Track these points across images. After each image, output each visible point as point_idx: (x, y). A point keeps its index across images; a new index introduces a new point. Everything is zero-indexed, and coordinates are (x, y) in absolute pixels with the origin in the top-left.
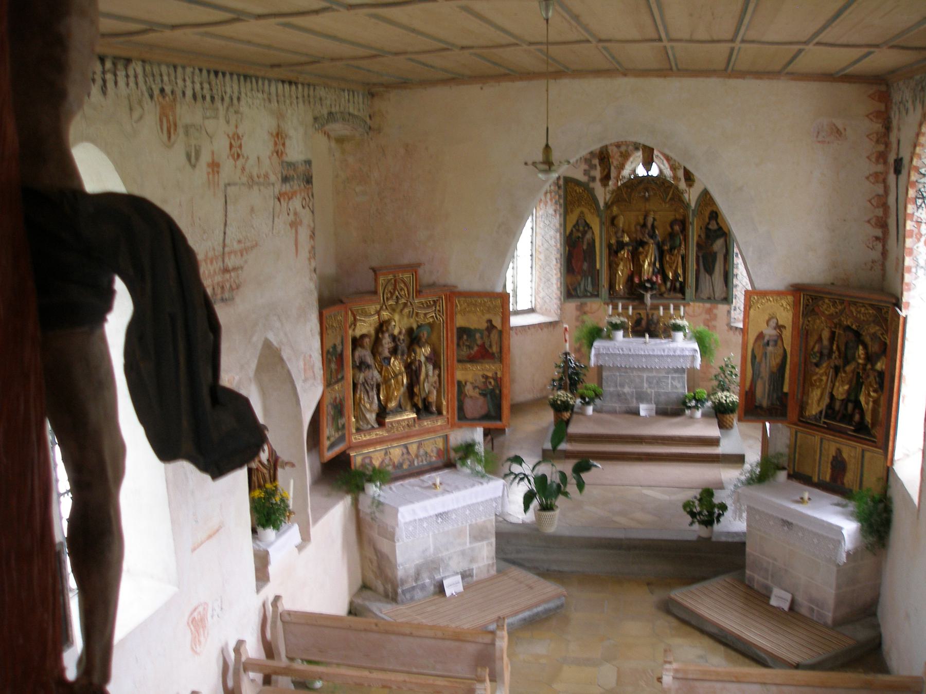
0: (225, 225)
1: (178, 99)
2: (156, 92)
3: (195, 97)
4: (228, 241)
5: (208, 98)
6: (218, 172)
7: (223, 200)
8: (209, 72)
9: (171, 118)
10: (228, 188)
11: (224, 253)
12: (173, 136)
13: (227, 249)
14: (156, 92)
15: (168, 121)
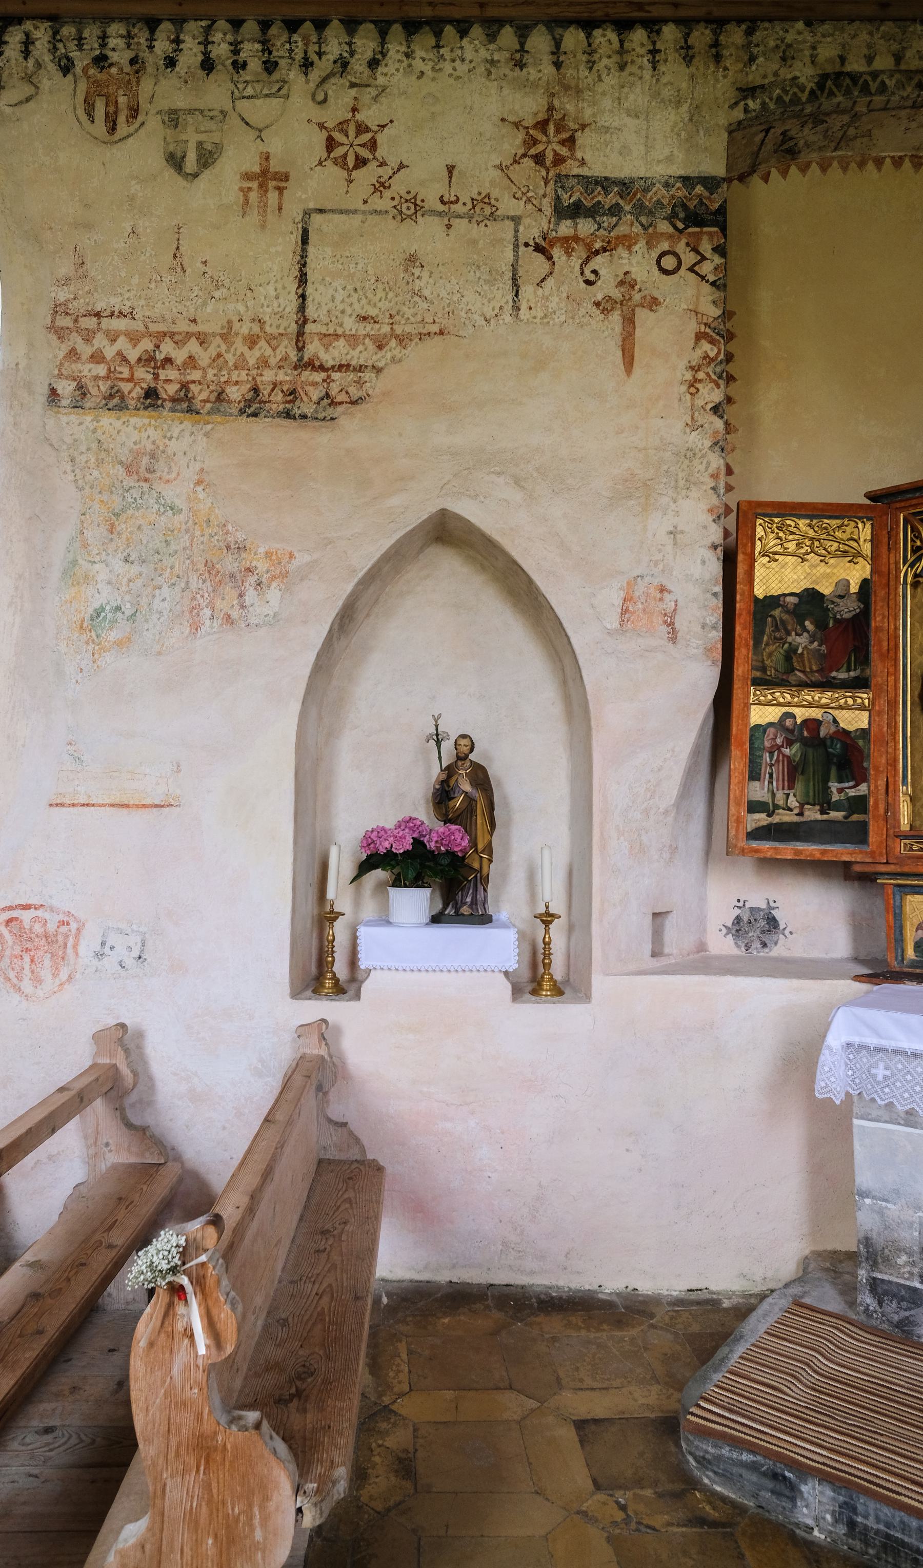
0: (303, 279)
1: (150, 70)
2: (81, 61)
3: (208, 65)
4: (310, 311)
5: (255, 65)
6: (280, 190)
7: (296, 237)
8: (265, 25)
9: (122, 100)
10: (317, 219)
11: (300, 334)
12: (123, 128)
13: (309, 327)
14: (81, 61)
15: (110, 101)
